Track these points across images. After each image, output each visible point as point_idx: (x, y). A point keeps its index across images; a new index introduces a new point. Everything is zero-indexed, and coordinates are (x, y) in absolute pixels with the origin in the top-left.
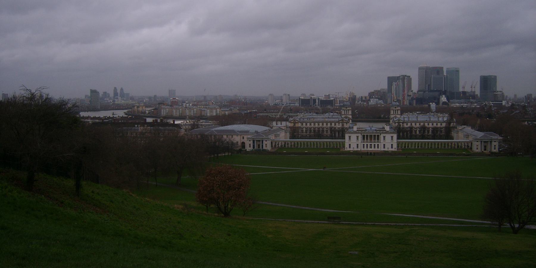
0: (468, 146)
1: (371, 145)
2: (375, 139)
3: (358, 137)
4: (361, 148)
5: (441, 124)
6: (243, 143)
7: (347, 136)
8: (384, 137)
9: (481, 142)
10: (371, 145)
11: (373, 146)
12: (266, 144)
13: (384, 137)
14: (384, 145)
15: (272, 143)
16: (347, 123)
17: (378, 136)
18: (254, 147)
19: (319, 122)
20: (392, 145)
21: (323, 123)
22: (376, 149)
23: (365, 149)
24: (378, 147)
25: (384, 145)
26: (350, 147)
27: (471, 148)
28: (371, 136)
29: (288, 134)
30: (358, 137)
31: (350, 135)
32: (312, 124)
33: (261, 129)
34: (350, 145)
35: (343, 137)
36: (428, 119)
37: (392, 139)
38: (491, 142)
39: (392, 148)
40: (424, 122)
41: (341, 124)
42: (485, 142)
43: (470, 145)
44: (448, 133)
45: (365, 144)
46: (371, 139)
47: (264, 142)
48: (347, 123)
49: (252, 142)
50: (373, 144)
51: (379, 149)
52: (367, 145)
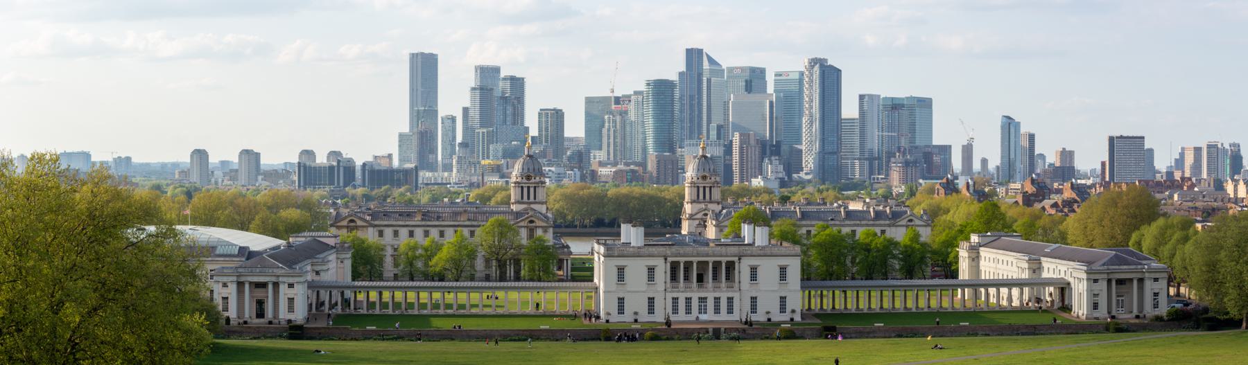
1: (703, 300)
2: (716, 277)
3: (651, 270)
5: (883, 232)
9: (1109, 281)
10: (703, 300)
11: (710, 304)
12: (291, 300)
14: (754, 299)
16: (545, 230)
17: (730, 266)
20: (783, 299)
22: (723, 316)
23: (682, 316)
24: (730, 311)
25: (754, 299)
26: (621, 310)
27: (1066, 308)
28: (703, 265)
30: (651, 270)
32: (419, 232)
38: (1141, 280)
39: (783, 309)
42: (1120, 282)
43: (1049, 294)
45: (682, 298)
46: (700, 279)
47: (283, 289)
48: (545, 230)
50: (711, 298)
51: (735, 316)
52: (688, 300)
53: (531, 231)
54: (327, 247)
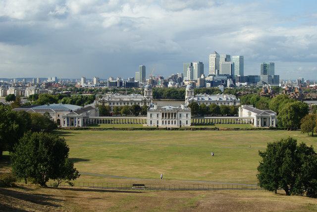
0: (251, 122)
1: (169, 121)
2: (172, 116)
3: (158, 115)
4: (160, 125)
6: (59, 120)
7: (149, 114)
8: (180, 115)
9: (262, 118)
10: (169, 121)
13: (180, 115)
15: (84, 120)
16: (148, 103)
17: (175, 114)
18: (68, 125)
19: (125, 102)
20: (187, 121)
21: (128, 102)
24: (175, 123)
26: (151, 123)
29: (98, 112)
31: (151, 113)
33: (75, 107)
34: (151, 121)
35: (145, 114)
36: (218, 99)
37: (187, 116)
39: (187, 123)
40: (214, 101)
41: (143, 104)
42: (264, 118)
44: (235, 112)
46: (169, 117)
48: (148, 103)
49: (66, 120)
52: (166, 121)
53: (145, 103)
54: (93, 108)
